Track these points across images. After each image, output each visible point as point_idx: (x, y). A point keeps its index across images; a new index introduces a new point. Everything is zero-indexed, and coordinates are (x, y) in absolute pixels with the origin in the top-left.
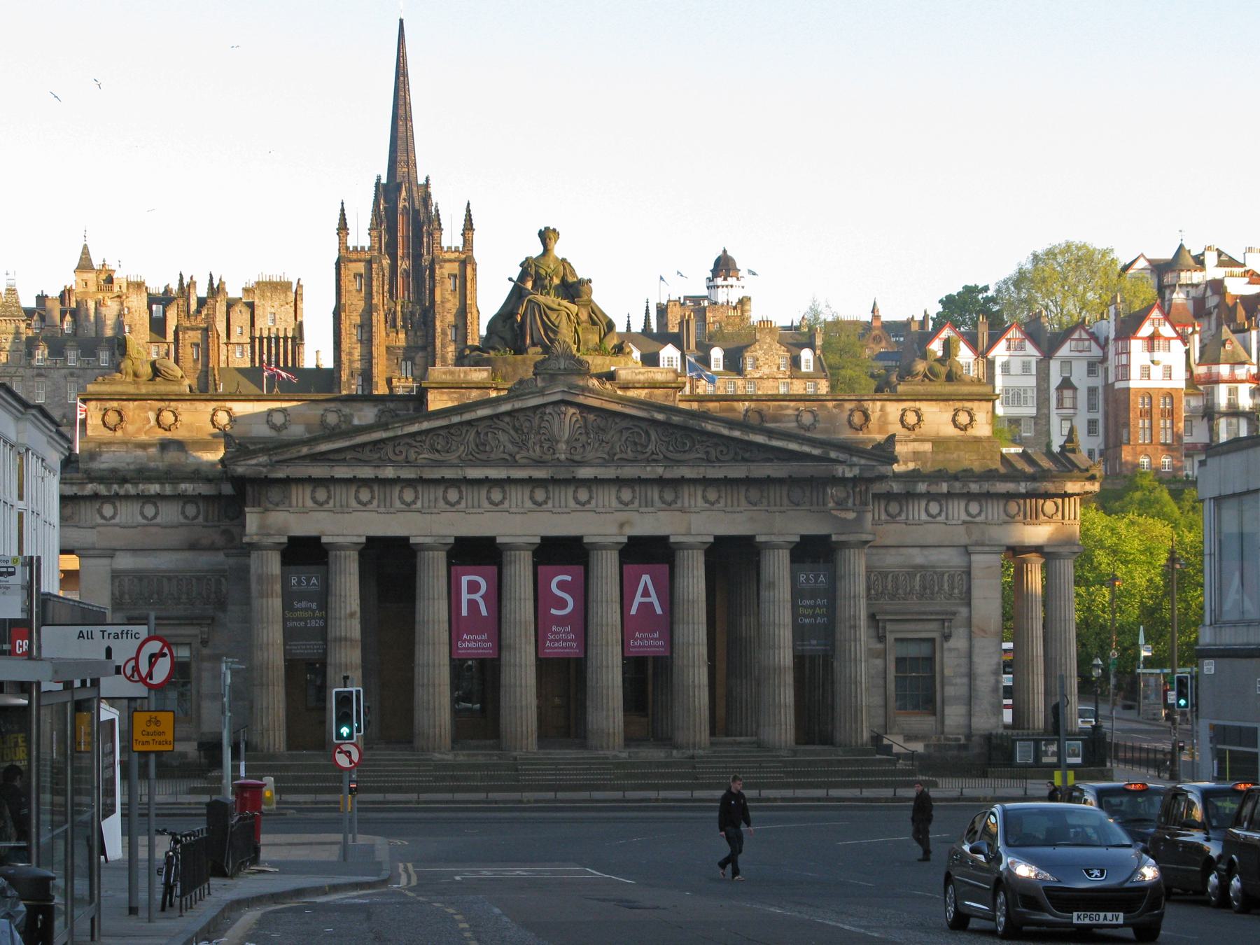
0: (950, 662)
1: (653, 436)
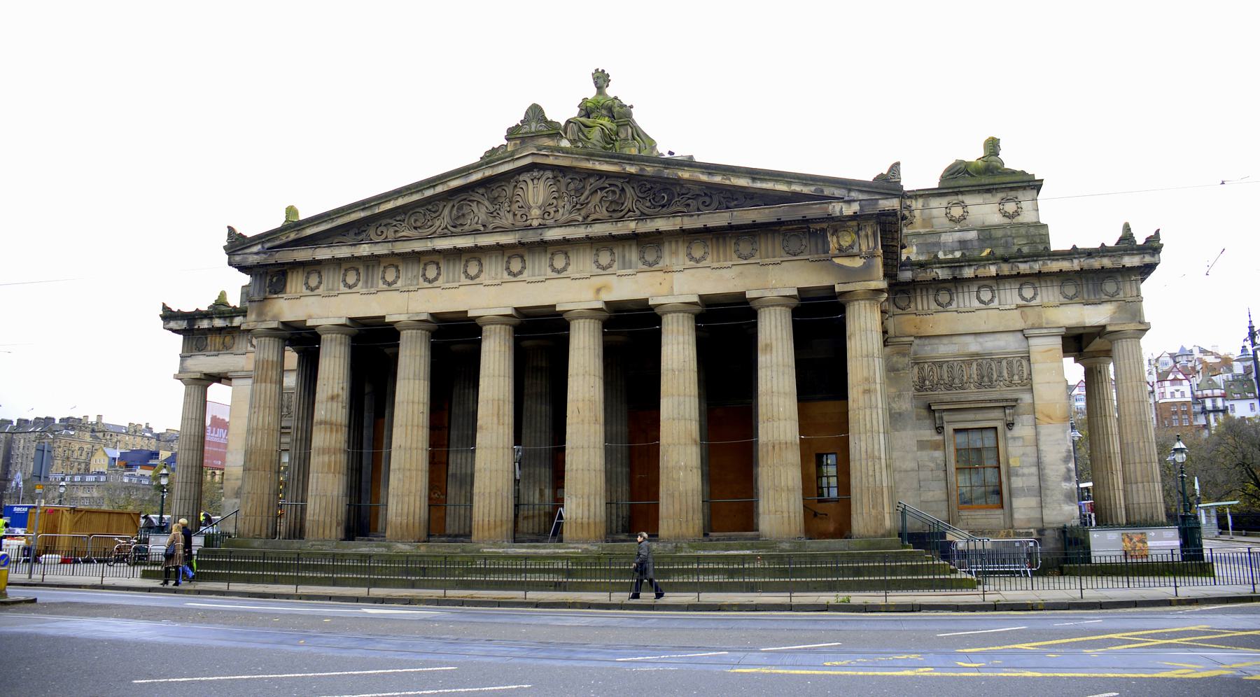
0: (1016, 450)
1: (629, 191)
